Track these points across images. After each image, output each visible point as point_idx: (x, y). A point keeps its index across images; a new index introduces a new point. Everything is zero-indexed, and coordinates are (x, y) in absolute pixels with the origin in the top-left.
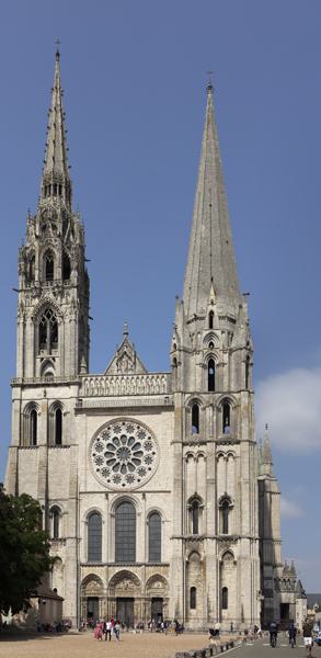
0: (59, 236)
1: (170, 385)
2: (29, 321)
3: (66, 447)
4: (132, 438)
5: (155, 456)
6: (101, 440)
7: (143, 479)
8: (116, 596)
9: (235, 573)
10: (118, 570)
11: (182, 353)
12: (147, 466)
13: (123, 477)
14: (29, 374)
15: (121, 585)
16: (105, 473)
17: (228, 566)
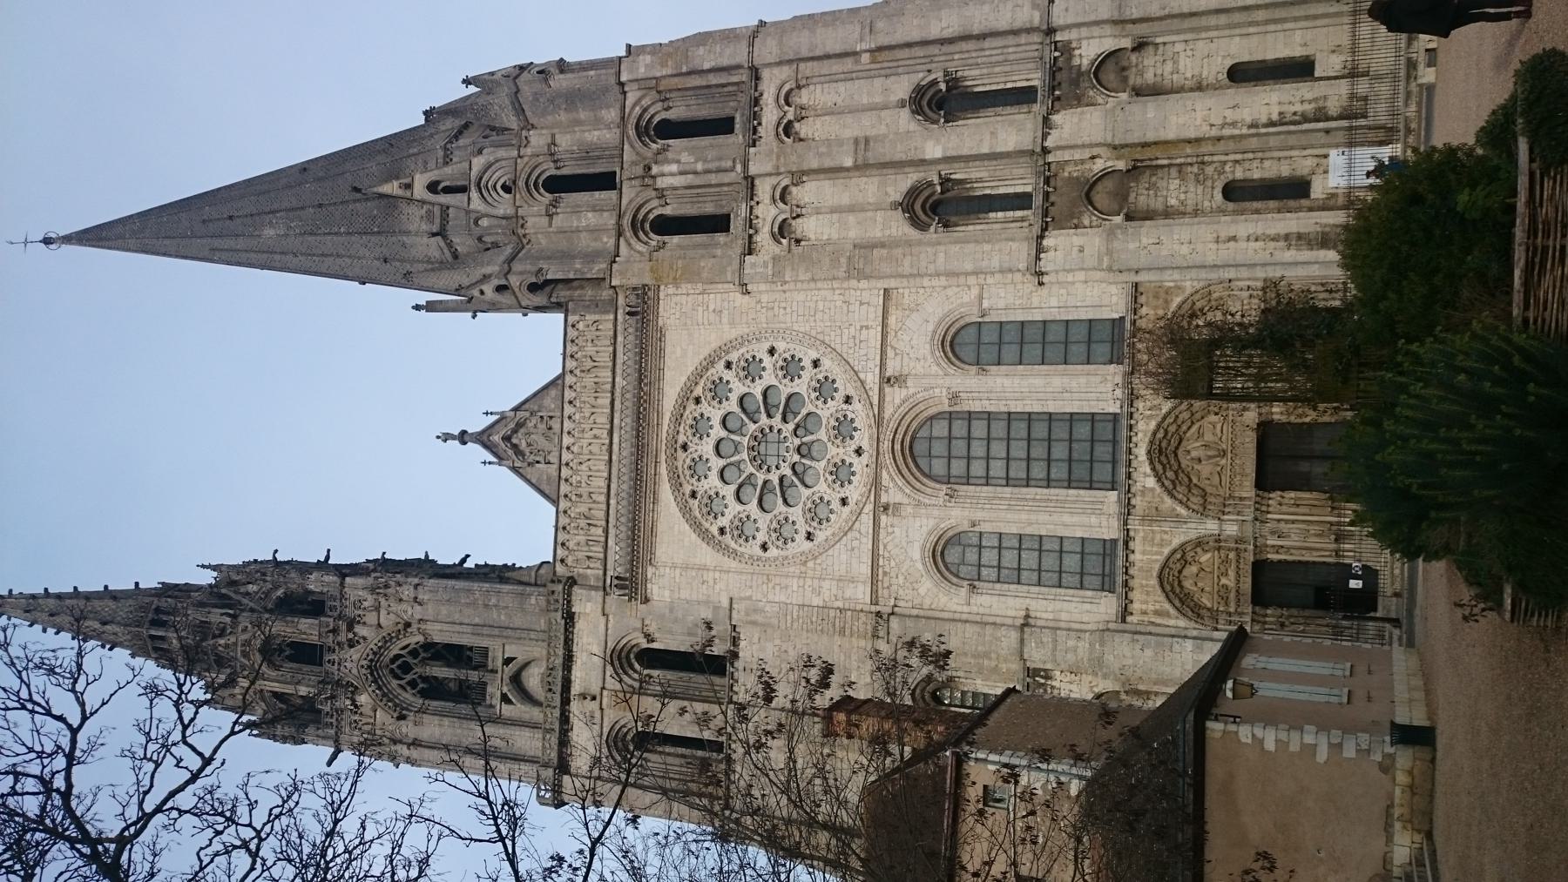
0: (234, 617)
1: (596, 306)
2: (408, 729)
3: (735, 641)
4: (724, 422)
5: (780, 346)
6: (723, 521)
7: (844, 386)
8: (1248, 490)
9: (1175, 43)
10: (1145, 479)
11: (517, 266)
12: (806, 375)
13: (835, 452)
14: (527, 742)
15: (1205, 469)
16: (817, 513)
17: (1150, 68)
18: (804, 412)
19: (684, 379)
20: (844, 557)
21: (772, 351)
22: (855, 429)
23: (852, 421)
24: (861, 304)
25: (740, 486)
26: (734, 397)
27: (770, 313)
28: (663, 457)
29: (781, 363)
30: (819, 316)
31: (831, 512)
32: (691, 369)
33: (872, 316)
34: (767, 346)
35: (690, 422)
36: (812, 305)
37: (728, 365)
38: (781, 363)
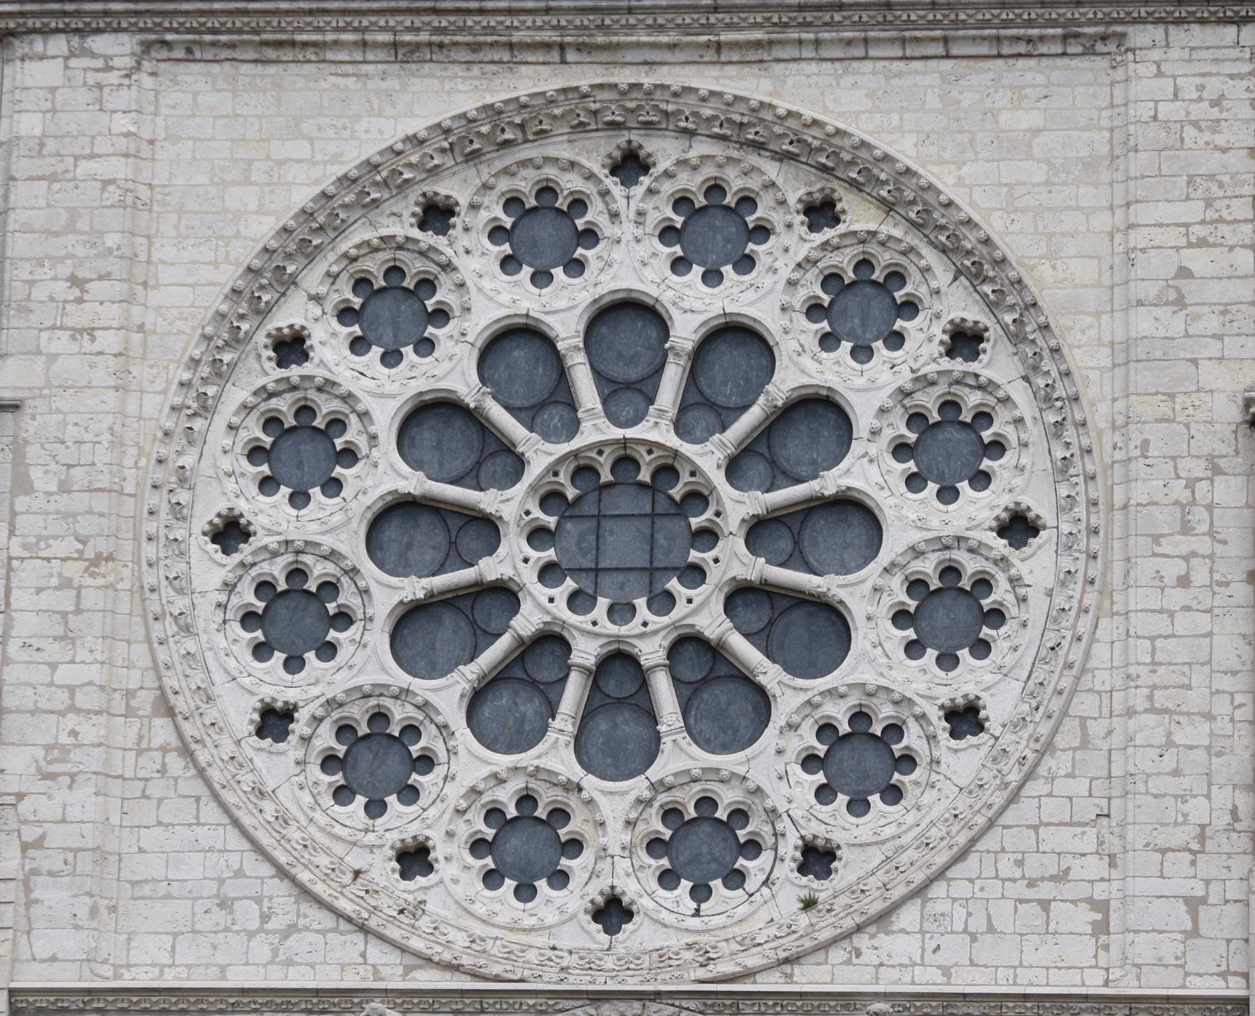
4: (734, 335)
7: (868, 838)
18: (770, 674)
19: (905, 151)
20: (193, 868)
21: (1018, 527)
22: (701, 892)
23: (735, 879)
24: (1194, 904)
25: (473, 417)
26: (832, 370)
27: (1165, 519)
28: (584, 76)
29: (971, 566)
30: (1149, 728)
31: (375, 808)
32: (946, 181)
33: (1143, 948)
34: (1040, 506)
35: (736, 184)
36: (1196, 699)
37: (964, 341)
38: (971, 566)
